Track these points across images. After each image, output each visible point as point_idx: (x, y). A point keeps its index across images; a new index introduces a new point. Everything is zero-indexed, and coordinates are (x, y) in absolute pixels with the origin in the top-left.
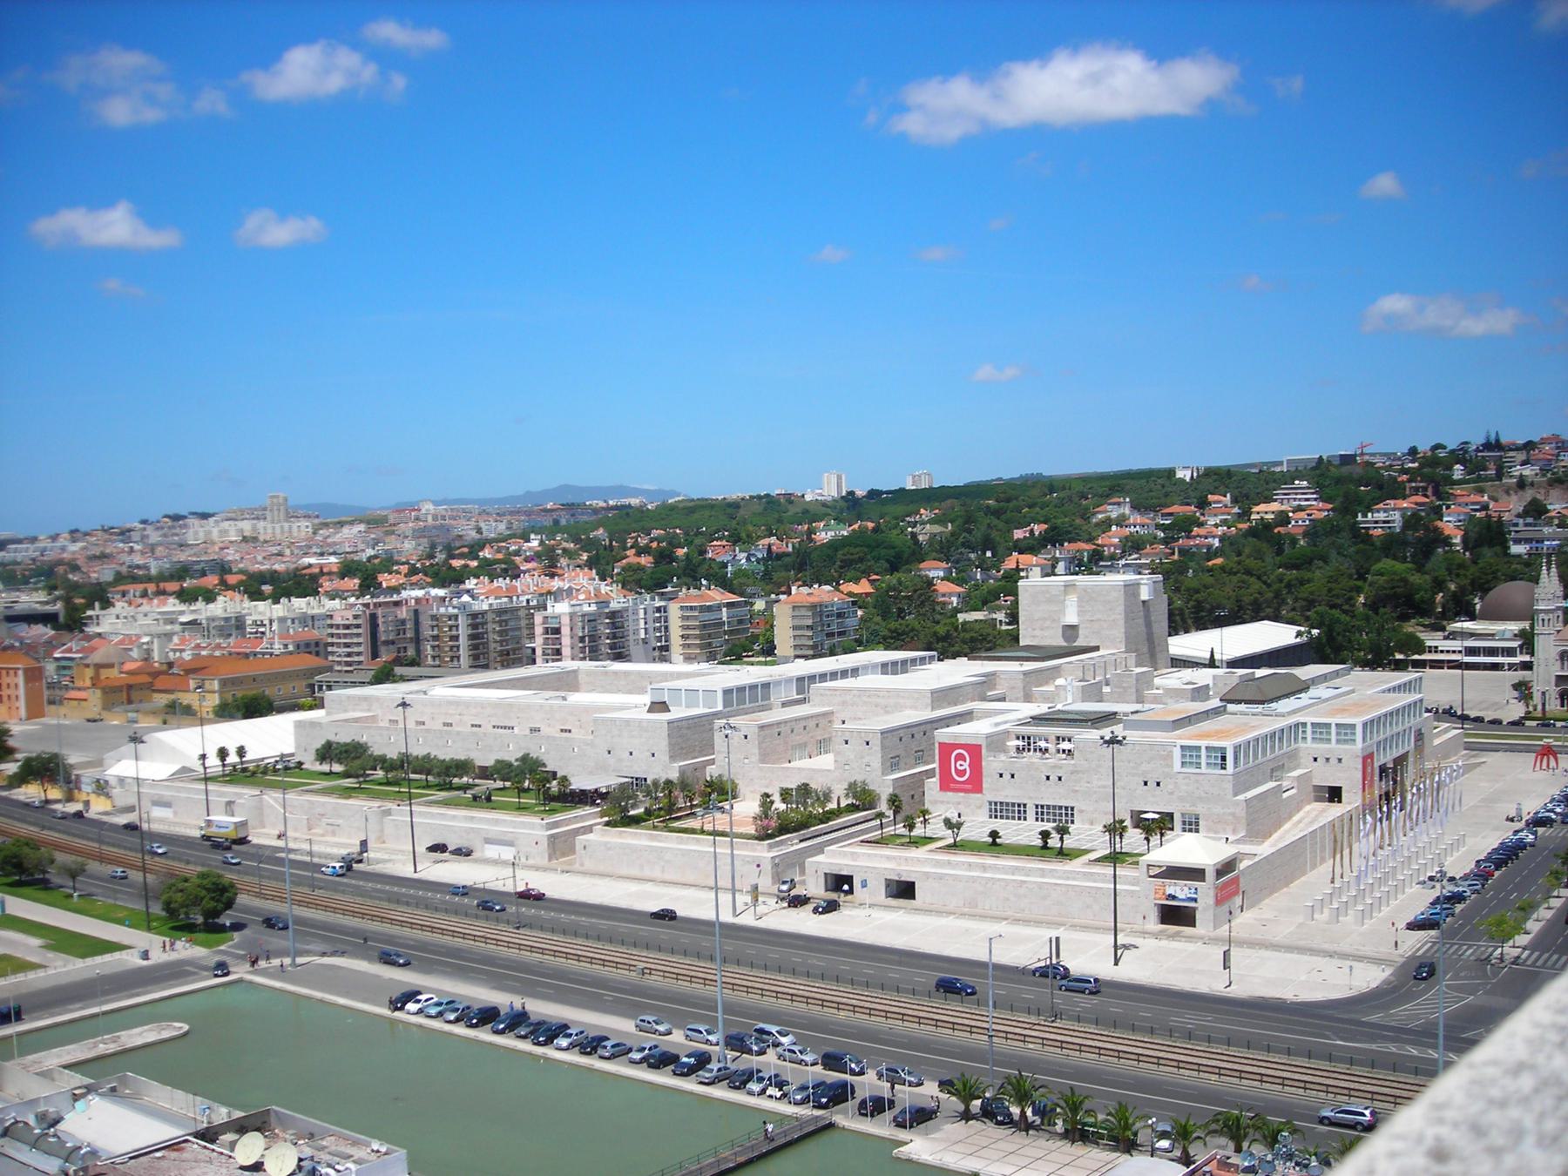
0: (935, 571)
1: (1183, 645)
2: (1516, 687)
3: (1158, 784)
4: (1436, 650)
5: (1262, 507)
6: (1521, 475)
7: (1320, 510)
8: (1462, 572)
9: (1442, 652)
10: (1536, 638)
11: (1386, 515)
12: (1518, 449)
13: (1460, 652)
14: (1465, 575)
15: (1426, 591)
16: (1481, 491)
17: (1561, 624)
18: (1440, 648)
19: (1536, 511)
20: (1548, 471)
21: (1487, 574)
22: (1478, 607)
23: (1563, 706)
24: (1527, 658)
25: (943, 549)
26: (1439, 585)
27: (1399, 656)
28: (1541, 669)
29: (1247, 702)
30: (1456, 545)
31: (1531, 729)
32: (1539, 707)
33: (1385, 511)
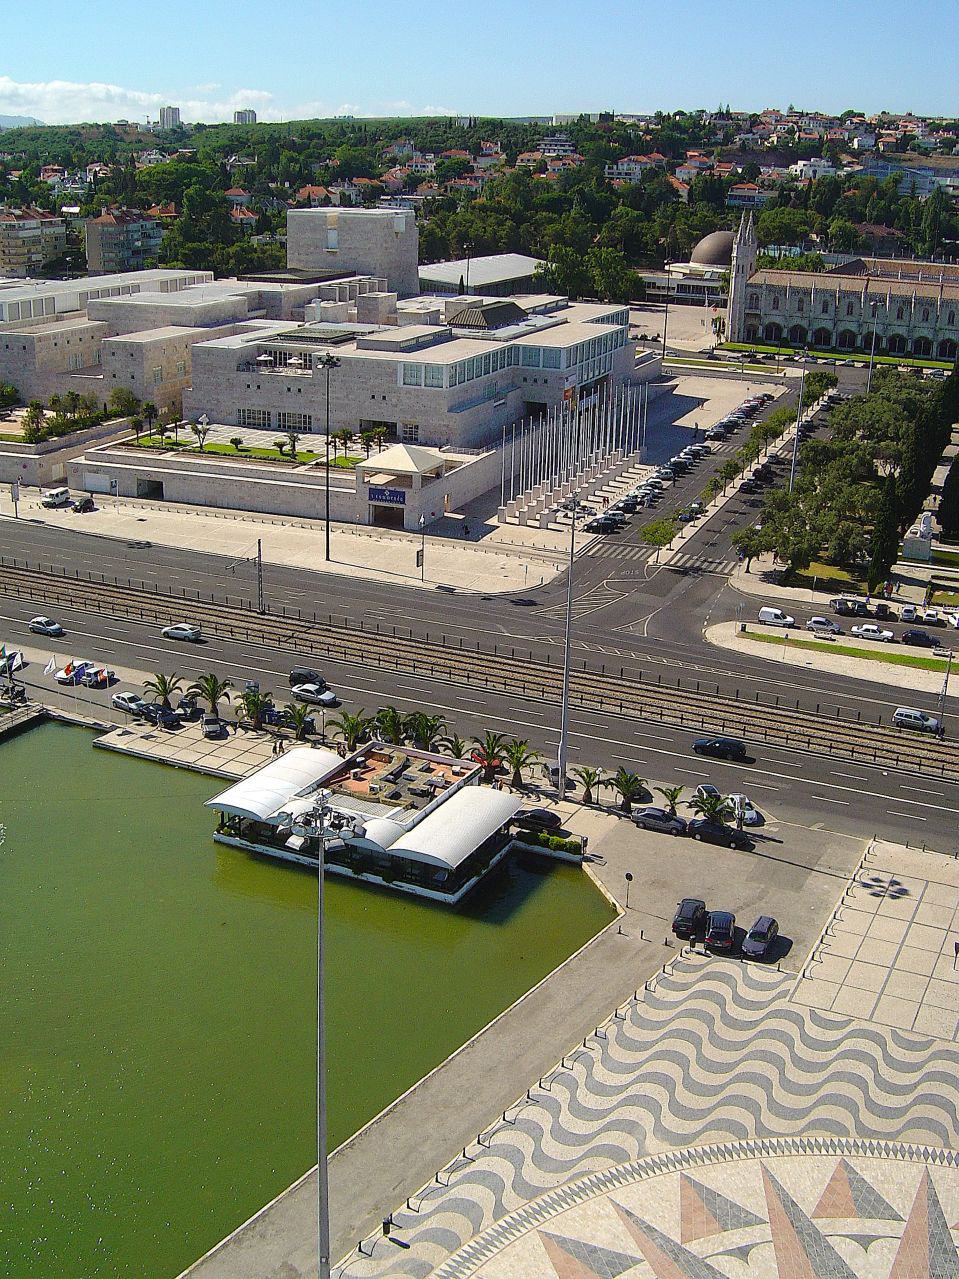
0: (237, 194)
1: (427, 272)
3: (384, 398)
5: (525, 156)
7: (574, 161)
13: (674, 289)
16: (709, 154)
25: (249, 177)
29: (470, 326)
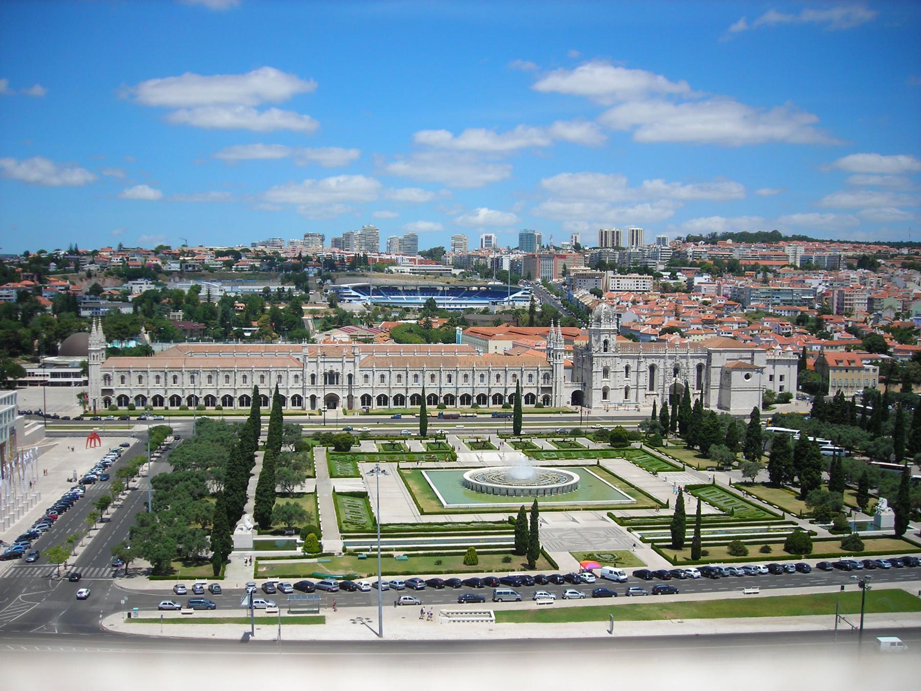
2: (80, 396)
4: (33, 374)
6: (89, 270)
8: (50, 327)
9: (37, 375)
10: (90, 367)
11: (7, 292)
12: (88, 254)
13: (48, 375)
14: (51, 329)
15: (28, 338)
16: (66, 279)
17: (104, 358)
18: (36, 374)
19: (96, 291)
20: (105, 268)
21: (64, 328)
22: (59, 348)
23: (106, 407)
24: (86, 378)
26: (36, 335)
27: (10, 379)
28: (94, 384)
30: (49, 310)
31: (87, 422)
32: (92, 408)
33: (7, 289)
